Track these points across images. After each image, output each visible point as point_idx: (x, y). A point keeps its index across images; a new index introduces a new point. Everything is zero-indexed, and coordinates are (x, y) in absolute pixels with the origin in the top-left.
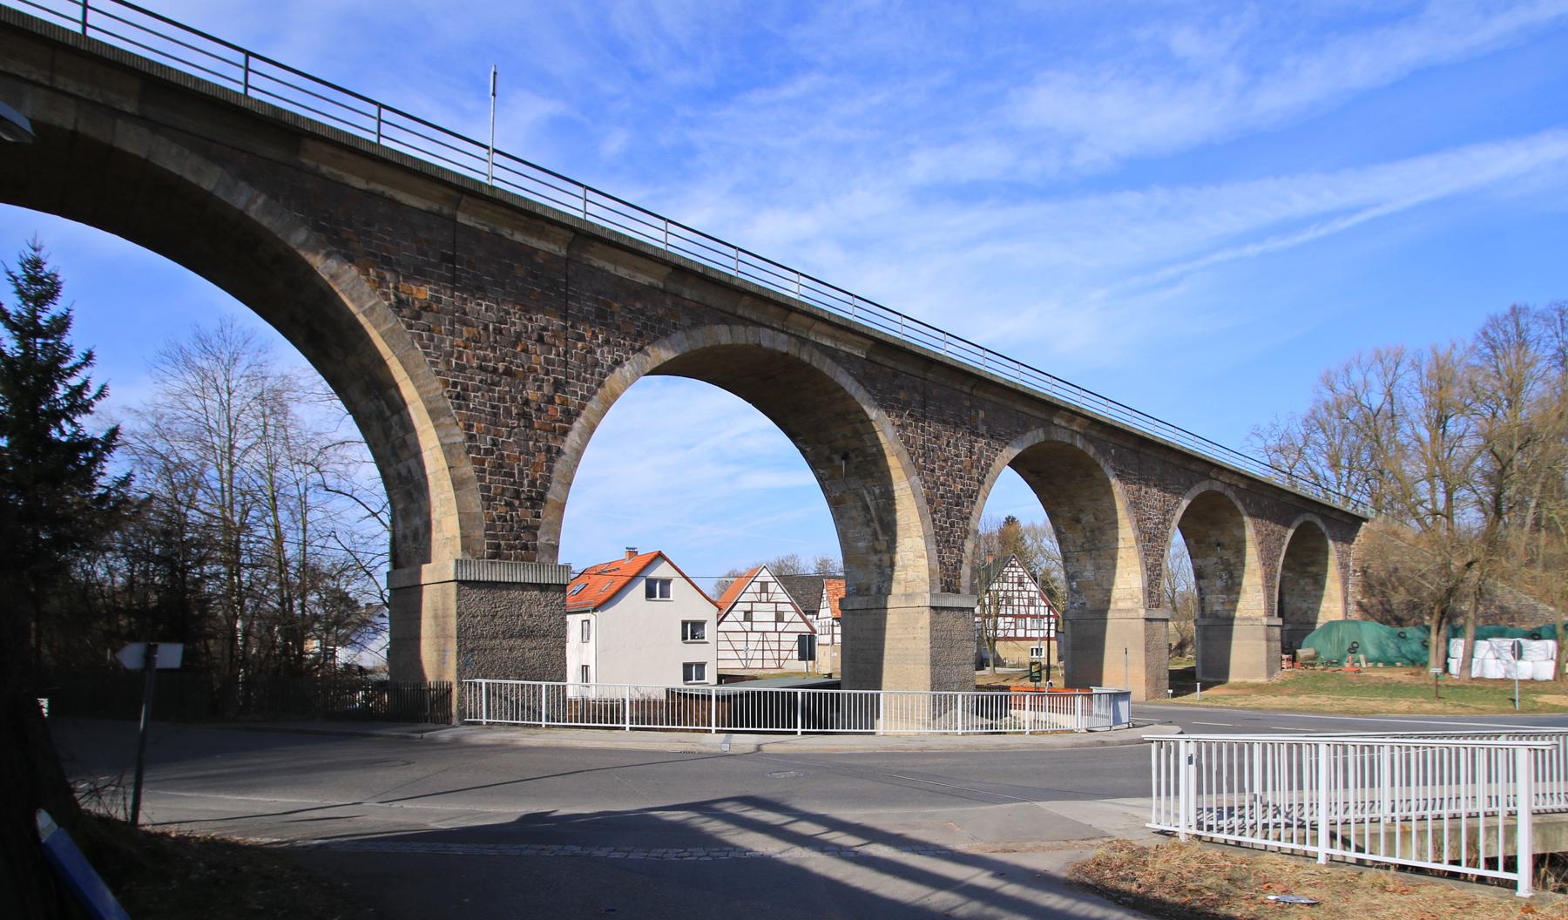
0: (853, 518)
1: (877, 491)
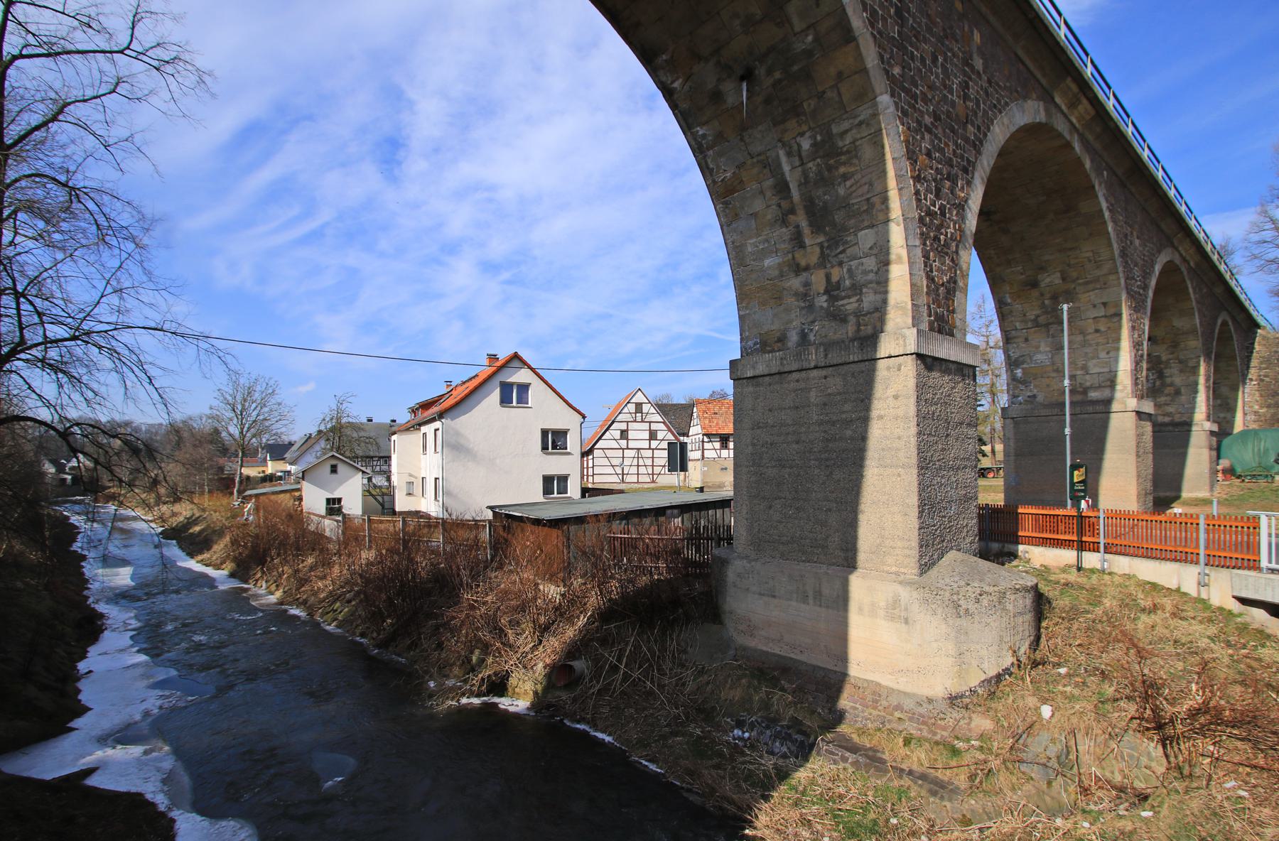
0: (754, 215)
1: (806, 144)
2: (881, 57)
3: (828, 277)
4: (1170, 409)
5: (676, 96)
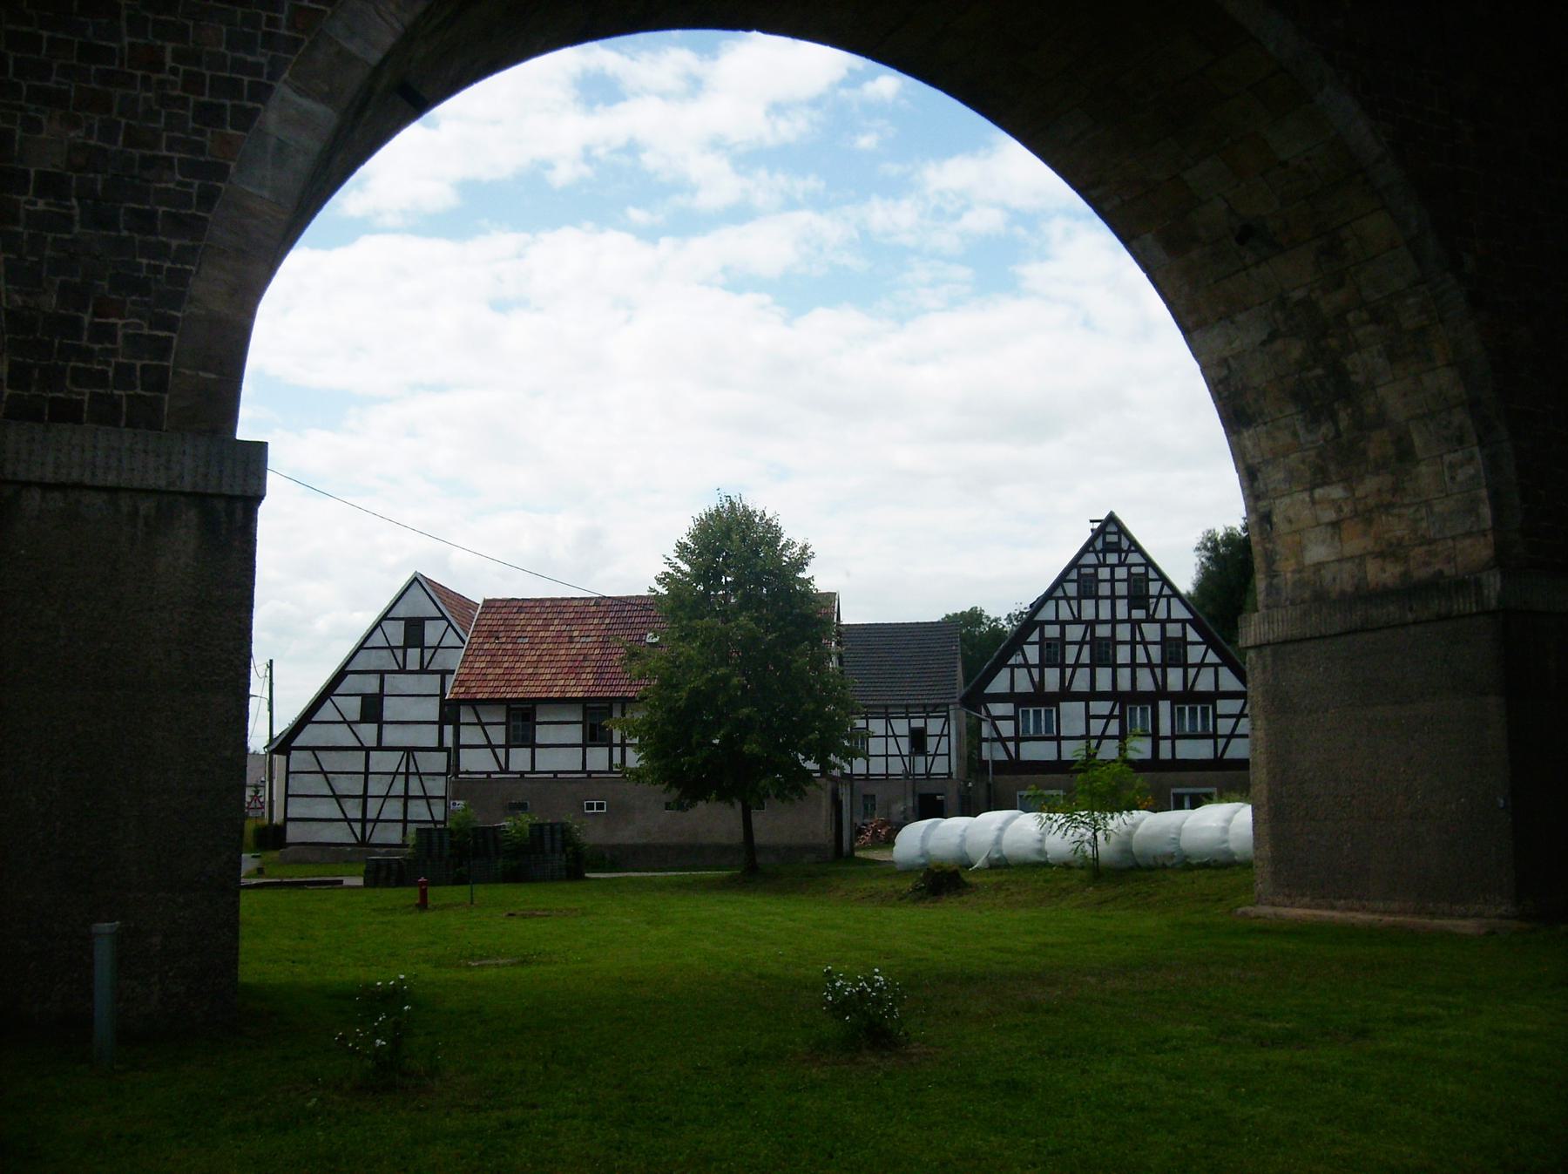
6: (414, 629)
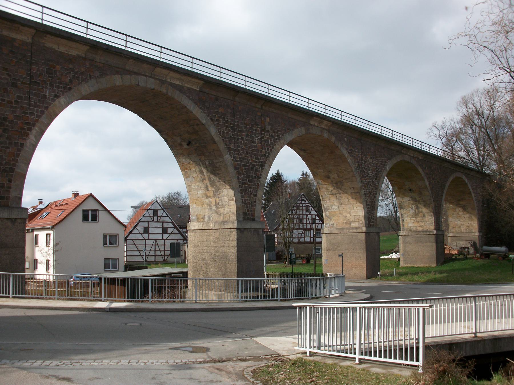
1: (207, 163)
2: (226, 145)
3: (216, 200)
4: (422, 224)
5: (168, 141)
6: (156, 212)
